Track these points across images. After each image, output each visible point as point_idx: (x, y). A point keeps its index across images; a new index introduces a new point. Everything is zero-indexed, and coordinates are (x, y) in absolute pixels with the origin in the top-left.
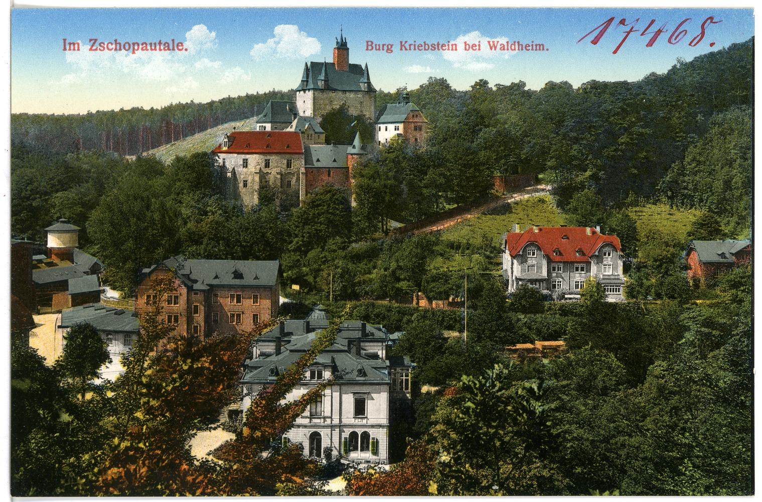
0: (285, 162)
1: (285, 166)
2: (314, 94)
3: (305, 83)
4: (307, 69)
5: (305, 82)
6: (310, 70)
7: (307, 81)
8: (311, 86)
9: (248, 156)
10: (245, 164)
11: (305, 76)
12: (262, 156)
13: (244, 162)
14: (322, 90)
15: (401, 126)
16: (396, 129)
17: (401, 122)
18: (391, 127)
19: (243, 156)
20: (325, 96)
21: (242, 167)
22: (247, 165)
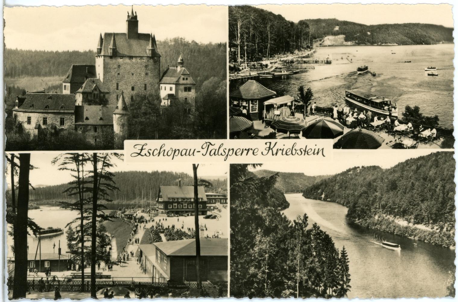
0: (59, 120)
1: (58, 124)
2: (104, 60)
3: (99, 51)
4: (101, 39)
5: (100, 50)
6: (104, 40)
7: (101, 49)
8: (102, 53)
9: (31, 115)
10: (29, 121)
11: (99, 44)
12: (41, 115)
13: (28, 120)
14: (111, 57)
15: (174, 86)
16: (171, 89)
17: (173, 84)
18: (168, 86)
19: (27, 115)
20: (114, 61)
21: (26, 123)
22: (30, 122)
